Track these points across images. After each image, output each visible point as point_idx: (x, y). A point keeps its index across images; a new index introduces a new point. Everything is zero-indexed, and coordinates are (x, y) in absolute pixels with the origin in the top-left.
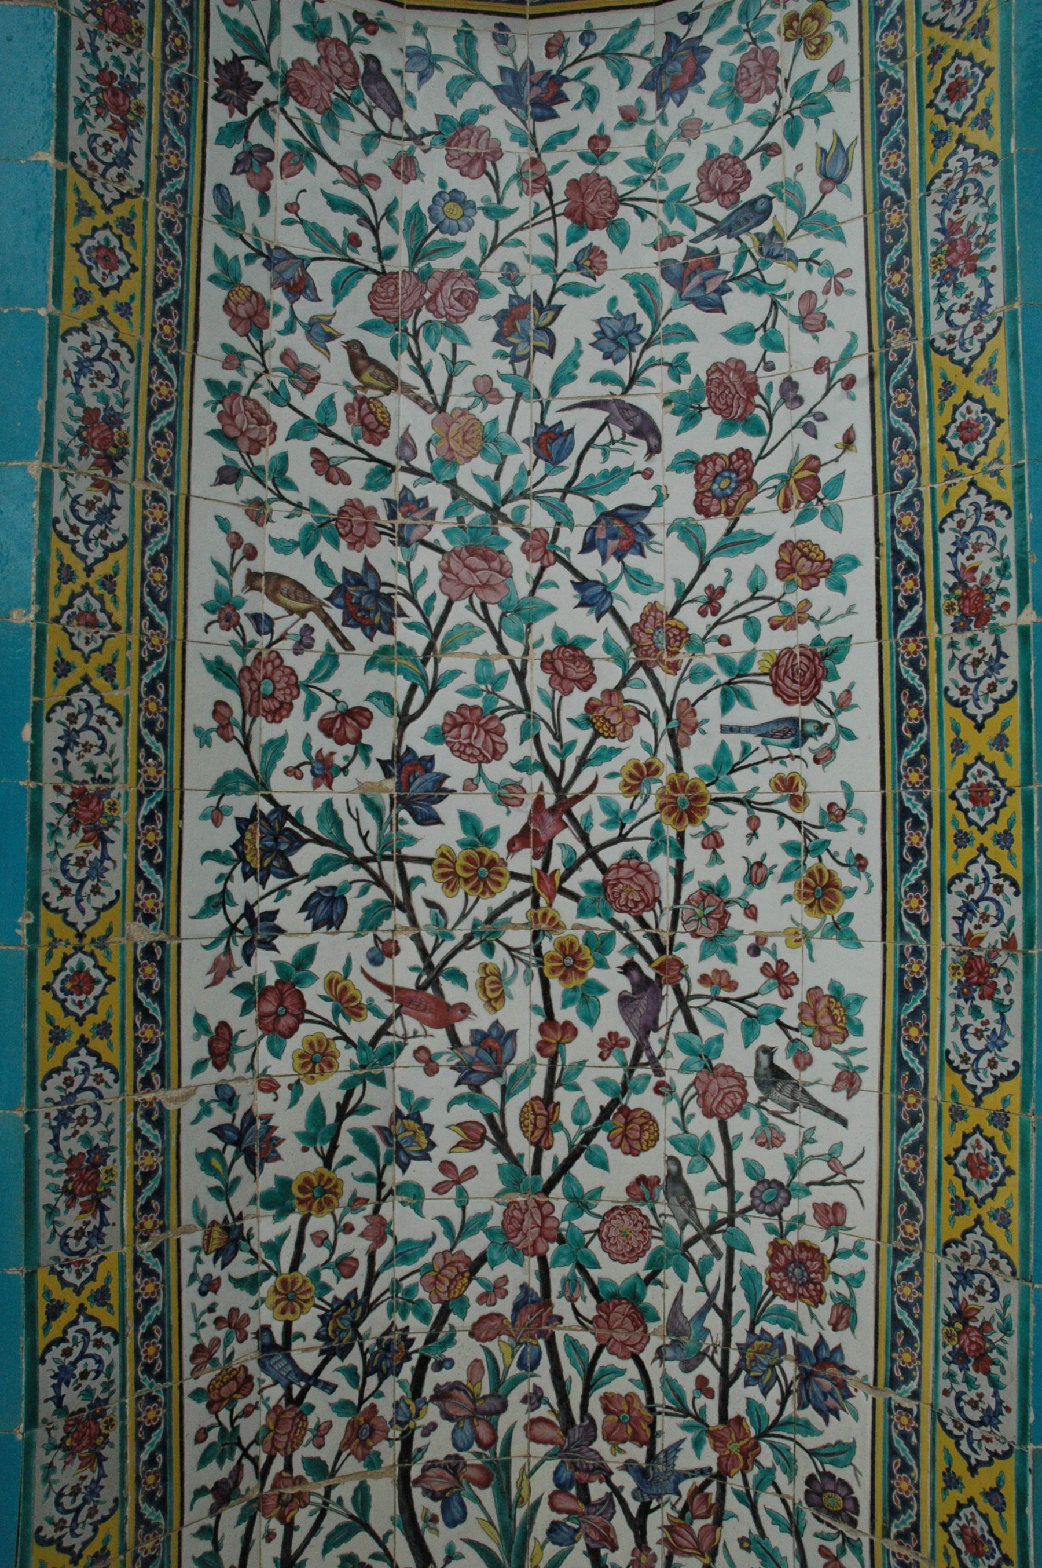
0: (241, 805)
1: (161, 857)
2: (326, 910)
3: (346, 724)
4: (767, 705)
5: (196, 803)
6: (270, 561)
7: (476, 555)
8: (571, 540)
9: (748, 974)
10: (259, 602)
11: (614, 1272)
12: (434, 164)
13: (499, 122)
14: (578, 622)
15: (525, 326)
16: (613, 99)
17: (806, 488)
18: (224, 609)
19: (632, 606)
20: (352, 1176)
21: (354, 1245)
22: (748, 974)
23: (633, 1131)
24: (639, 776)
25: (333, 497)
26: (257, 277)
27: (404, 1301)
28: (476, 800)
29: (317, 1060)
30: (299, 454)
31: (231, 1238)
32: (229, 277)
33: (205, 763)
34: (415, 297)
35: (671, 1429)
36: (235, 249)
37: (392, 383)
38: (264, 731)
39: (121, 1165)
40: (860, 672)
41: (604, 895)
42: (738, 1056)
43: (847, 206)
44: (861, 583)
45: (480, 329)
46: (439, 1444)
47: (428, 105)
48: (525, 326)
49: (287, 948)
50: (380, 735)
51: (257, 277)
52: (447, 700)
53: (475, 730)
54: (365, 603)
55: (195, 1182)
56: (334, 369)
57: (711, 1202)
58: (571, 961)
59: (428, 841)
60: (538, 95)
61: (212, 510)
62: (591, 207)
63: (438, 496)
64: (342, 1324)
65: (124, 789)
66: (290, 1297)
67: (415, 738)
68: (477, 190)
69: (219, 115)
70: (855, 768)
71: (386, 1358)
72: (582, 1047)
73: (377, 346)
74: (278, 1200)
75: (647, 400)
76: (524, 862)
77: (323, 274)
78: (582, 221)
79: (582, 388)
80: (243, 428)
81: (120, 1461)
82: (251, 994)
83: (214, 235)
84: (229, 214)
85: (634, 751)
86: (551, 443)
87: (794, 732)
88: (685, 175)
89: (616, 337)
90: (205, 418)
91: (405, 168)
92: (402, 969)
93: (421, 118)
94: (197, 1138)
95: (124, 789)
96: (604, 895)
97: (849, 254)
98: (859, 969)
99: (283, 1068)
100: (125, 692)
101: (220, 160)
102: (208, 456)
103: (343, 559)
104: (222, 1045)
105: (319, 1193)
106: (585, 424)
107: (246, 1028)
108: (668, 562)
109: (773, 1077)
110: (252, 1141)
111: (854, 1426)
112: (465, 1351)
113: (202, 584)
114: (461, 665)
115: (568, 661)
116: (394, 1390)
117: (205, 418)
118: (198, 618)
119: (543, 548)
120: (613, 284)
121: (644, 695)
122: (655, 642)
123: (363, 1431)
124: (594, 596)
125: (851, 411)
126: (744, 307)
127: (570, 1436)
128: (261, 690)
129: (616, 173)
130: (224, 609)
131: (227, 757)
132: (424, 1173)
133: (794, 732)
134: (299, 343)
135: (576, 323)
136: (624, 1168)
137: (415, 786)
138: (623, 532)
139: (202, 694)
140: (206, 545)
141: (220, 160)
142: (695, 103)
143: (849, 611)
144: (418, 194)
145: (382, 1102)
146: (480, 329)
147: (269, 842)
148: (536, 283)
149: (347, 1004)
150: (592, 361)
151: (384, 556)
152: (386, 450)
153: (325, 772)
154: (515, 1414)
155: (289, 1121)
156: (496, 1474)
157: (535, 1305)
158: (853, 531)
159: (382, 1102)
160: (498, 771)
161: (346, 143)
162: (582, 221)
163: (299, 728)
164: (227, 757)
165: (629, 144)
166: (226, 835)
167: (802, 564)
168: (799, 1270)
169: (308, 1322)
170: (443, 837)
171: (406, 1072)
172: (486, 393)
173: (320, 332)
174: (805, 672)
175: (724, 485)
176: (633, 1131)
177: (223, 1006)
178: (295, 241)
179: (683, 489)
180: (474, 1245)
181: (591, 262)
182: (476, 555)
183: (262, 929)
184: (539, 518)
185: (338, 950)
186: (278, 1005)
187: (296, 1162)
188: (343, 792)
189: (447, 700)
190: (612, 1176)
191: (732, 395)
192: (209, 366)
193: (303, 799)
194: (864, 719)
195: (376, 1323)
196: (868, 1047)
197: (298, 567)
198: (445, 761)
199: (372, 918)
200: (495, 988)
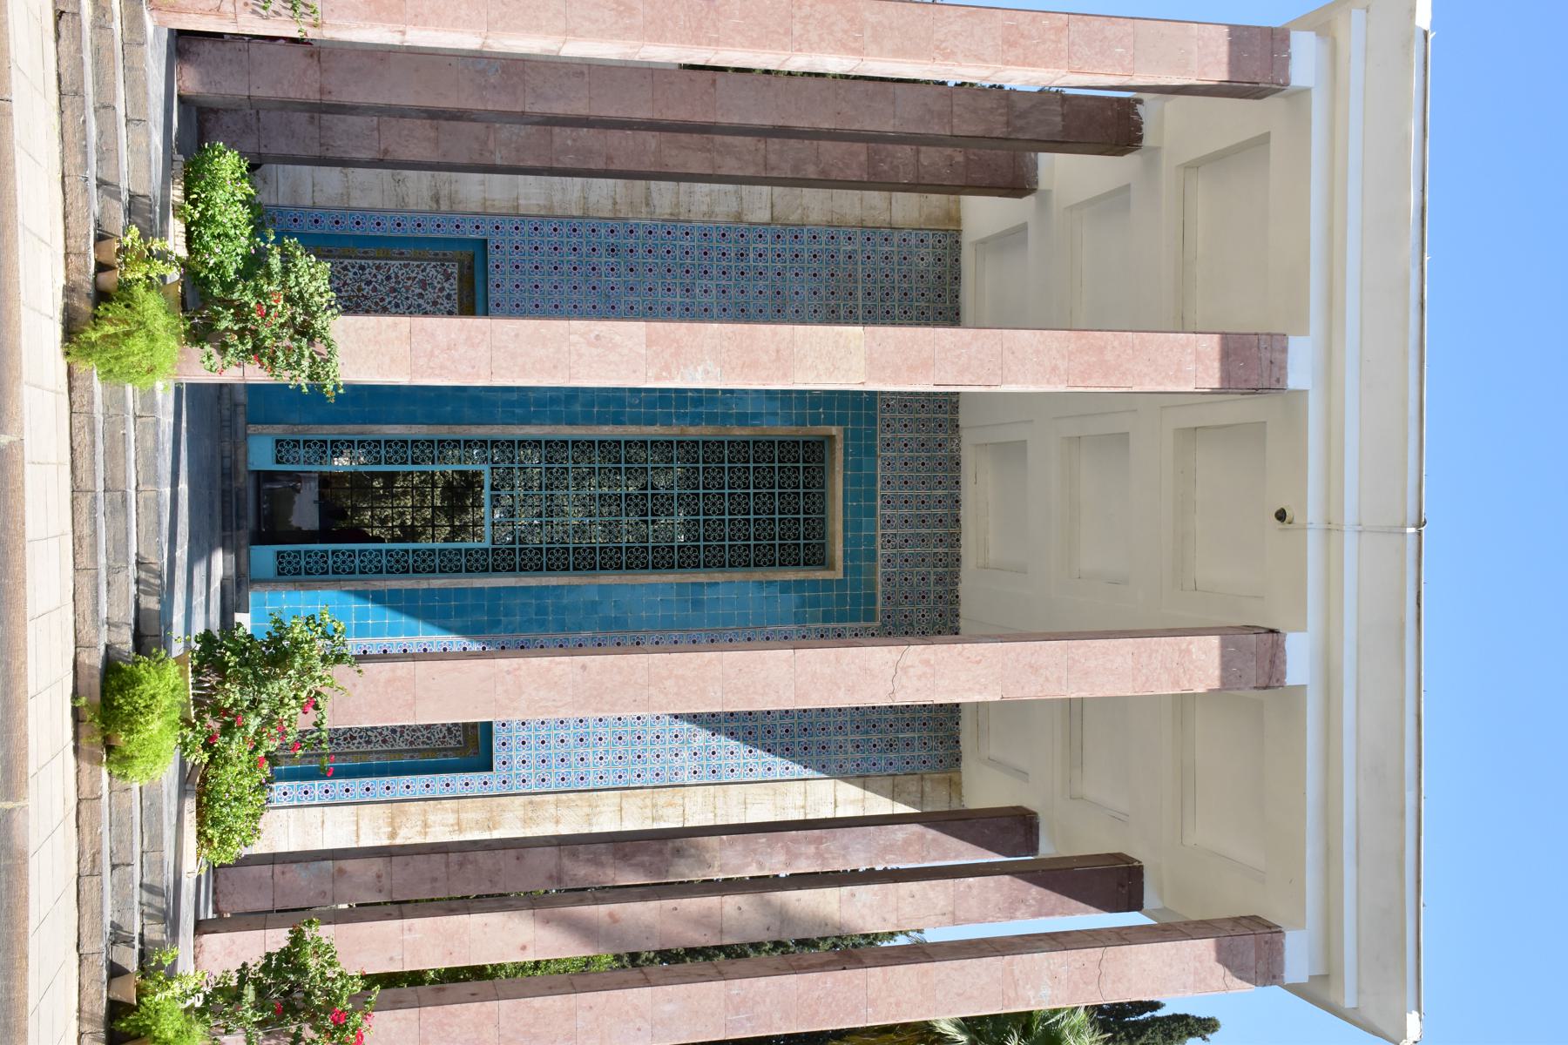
7: (394, 290)
15: (421, 296)
28: (367, 290)
34: (424, 284)
47: (446, 285)
48: (421, 296)
53: (375, 289)
54: (388, 278)
60: (449, 297)
80: (406, 266)
115: (382, 300)
128: (378, 268)
137: (369, 283)
182: (394, 290)
185: (351, 275)
186: (345, 268)
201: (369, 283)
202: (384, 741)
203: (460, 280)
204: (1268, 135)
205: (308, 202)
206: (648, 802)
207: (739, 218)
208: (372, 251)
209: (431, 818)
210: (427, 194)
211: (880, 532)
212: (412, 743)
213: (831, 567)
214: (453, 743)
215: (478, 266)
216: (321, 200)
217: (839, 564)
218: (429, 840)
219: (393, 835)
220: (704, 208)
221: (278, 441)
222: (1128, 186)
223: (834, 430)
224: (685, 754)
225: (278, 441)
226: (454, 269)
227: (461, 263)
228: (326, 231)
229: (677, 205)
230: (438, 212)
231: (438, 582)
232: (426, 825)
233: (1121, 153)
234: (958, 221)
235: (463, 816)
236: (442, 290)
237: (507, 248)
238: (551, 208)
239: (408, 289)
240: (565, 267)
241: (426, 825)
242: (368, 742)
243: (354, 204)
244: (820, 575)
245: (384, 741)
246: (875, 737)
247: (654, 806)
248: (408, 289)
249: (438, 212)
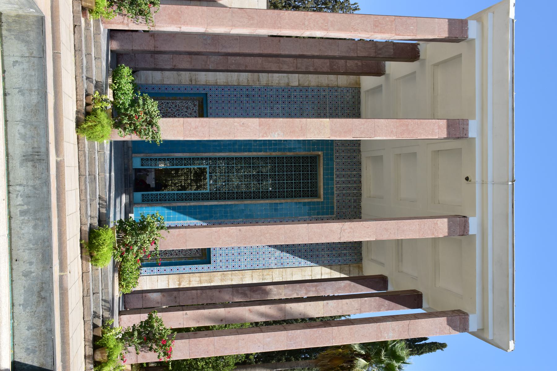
7: (178, 110)
15: (186, 112)
28: (169, 110)
34: (187, 108)
48: (186, 112)
53: (172, 110)
54: (176, 106)
60: (195, 112)
128: (173, 103)
137: (170, 108)
182: (178, 110)
201: (170, 108)
202: (176, 255)
203: (199, 106)
204: (461, 54)
205: (151, 82)
206: (261, 274)
207: (288, 84)
209: (192, 279)
210: (188, 79)
211: (335, 186)
213: (320, 197)
215: (204, 102)
216: (155, 82)
217: (322, 196)
218: (191, 286)
219: (180, 284)
220: (277, 82)
222: (415, 72)
223: (320, 153)
224: (273, 258)
226: (197, 103)
227: (199, 100)
228: (156, 92)
229: (268, 81)
230: (191, 84)
231: (193, 204)
232: (190, 281)
233: (413, 61)
234: (360, 84)
235: (202, 278)
236: (193, 109)
237: (214, 96)
238: (228, 82)
239: (182, 110)
240: (232, 102)
241: (190, 281)
242: (171, 255)
243: (165, 83)
244: (316, 200)
245: (176, 255)
246: (334, 252)
247: (263, 275)
248: (182, 110)
249: (191, 84)
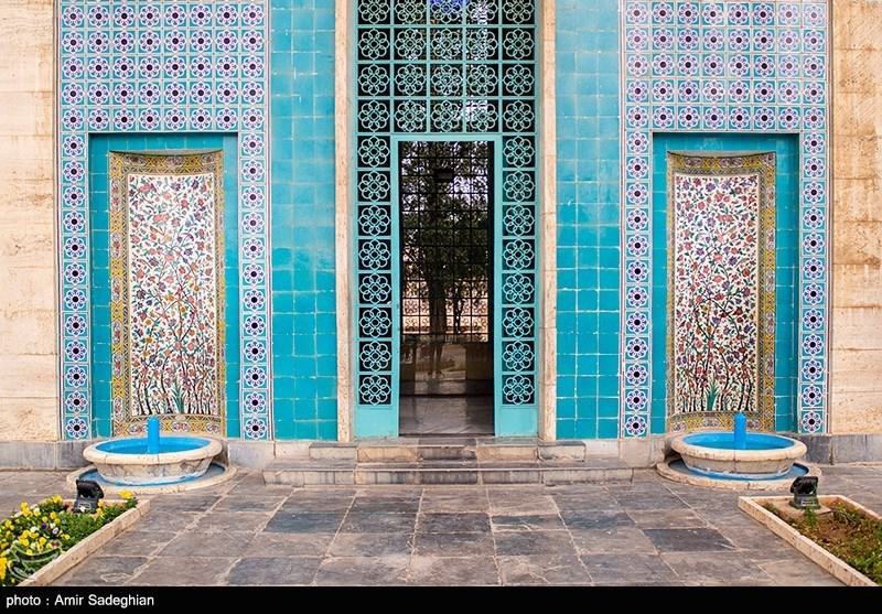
0: (137, 289)
1: (126, 296)
2: (150, 303)
3: (152, 278)
4: (205, 276)
5: (131, 289)
6: (140, 258)
8: (182, 253)
9: (204, 311)
10: (138, 263)
11: (190, 352)
12: (161, 198)
13: (172, 191)
14: (183, 264)
15: (175, 222)
16: (187, 188)
17: (209, 248)
18: (134, 264)
19: (190, 262)
20: (154, 338)
21: (154, 348)
22: (204, 311)
23: (192, 333)
24: (192, 285)
25: (149, 249)
26: (136, 219)
27: (162, 356)
29: (148, 323)
30: (143, 243)
31: (137, 345)
32: (132, 220)
33: (132, 284)
35: (198, 373)
36: (133, 216)
37: (157, 231)
38: (140, 280)
39: (122, 333)
40: (213, 272)
41: (187, 302)
42: (203, 322)
43: (213, 210)
44: (214, 260)
45: (169, 222)
46: (167, 376)
47: (160, 190)
48: (175, 222)
49: (144, 308)
50: (157, 280)
51: (136, 219)
52: (166, 275)
54: (154, 262)
55: (132, 337)
56: (148, 231)
57: (201, 342)
58: (183, 310)
59: (164, 294)
61: (131, 251)
62: (184, 205)
63: (164, 247)
64: (153, 358)
65: (121, 287)
66: (145, 354)
67: (161, 280)
68: (168, 202)
69: (130, 198)
70: (213, 285)
71: (158, 364)
72: (185, 321)
73: (154, 226)
74: (143, 341)
75: (192, 233)
76: (177, 296)
77: (146, 217)
78: (183, 207)
79: (183, 231)
81: (122, 371)
82: (139, 314)
83: (130, 215)
84: (132, 211)
85: (190, 282)
86: (179, 239)
87: (208, 279)
88: (196, 201)
89: (188, 224)
90: (130, 239)
91: (157, 199)
92: (161, 311)
93: (159, 192)
94: (132, 331)
95: (121, 287)
96: (187, 302)
97: (213, 217)
98: (214, 310)
99: (144, 323)
100: (121, 275)
101: (130, 204)
102: (131, 245)
103: (150, 257)
104: (135, 320)
105: (149, 340)
106: (184, 237)
107: (139, 318)
108: (194, 256)
109: (207, 324)
110: (140, 333)
111: (215, 368)
112: (170, 364)
113: (131, 262)
114: (168, 270)
115: (182, 270)
116: (160, 368)
117: (130, 239)
118: (130, 266)
119: (179, 254)
120: (187, 216)
121: (191, 274)
122: (193, 267)
123: (156, 374)
124: (185, 261)
125: (213, 238)
126: (203, 221)
127: (185, 375)
128: (140, 275)
129: (188, 200)
130: (134, 264)
131: (135, 283)
132: (164, 339)
133: (208, 279)
134: (143, 227)
135: (183, 222)
136: (191, 338)
137: (162, 287)
138: (189, 252)
139: (131, 275)
140: (131, 256)
141: (130, 204)
142: (197, 190)
143: (212, 264)
144: (159, 203)
145: (158, 329)
146: (169, 222)
147: (142, 294)
148: (177, 216)
149: (152, 315)
150: (185, 227)
151: (156, 256)
152: (156, 241)
153: (149, 285)
154: (178, 373)
155: (145, 331)
156: (175, 381)
157: (180, 357)
158: (213, 256)
159: (158, 329)
160: (173, 284)
161: (148, 198)
162: (183, 207)
163: (145, 279)
164: (135, 283)
165: (189, 195)
166: (135, 293)
167: (209, 258)
168: (210, 348)
169: (148, 357)
170: (166, 293)
171: (161, 325)
172: (170, 232)
173: (146, 225)
174: (209, 272)
175: (201, 246)
176: (192, 333)
177: (135, 315)
178: (142, 213)
179: (196, 246)
180: (171, 349)
181: (184, 213)
183: (141, 305)
184: (178, 250)
185: (151, 308)
186: (143, 315)
187: (146, 336)
188: (151, 288)
189: (166, 275)
190: (189, 339)
191: (201, 234)
192: (130, 233)
193: (146, 289)
194: (214, 278)
195: (157, 359)
196: (215, 319)
197: (144, 258)
198: (165, 283)
199: (156, 304)
200: (174, 314)
202: (746, 273)
208: (115, 280)
212: (751, 239)
214: (754, 188)
221: (362, 402)
225: (362, 402)
226: (138, 179)
231: (548, 202)
237: (99, 107)
242: (746, 293)
